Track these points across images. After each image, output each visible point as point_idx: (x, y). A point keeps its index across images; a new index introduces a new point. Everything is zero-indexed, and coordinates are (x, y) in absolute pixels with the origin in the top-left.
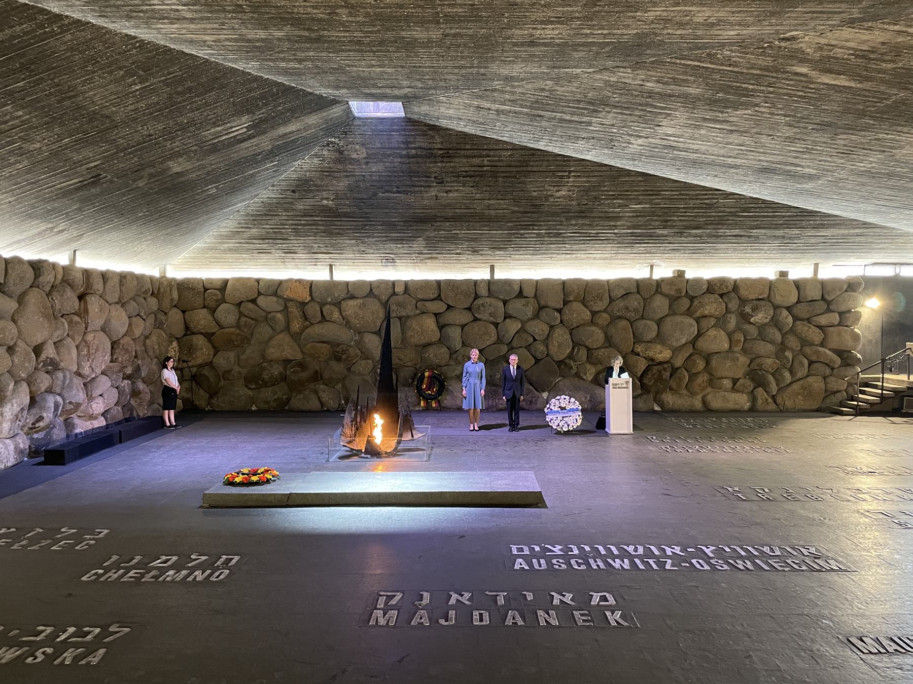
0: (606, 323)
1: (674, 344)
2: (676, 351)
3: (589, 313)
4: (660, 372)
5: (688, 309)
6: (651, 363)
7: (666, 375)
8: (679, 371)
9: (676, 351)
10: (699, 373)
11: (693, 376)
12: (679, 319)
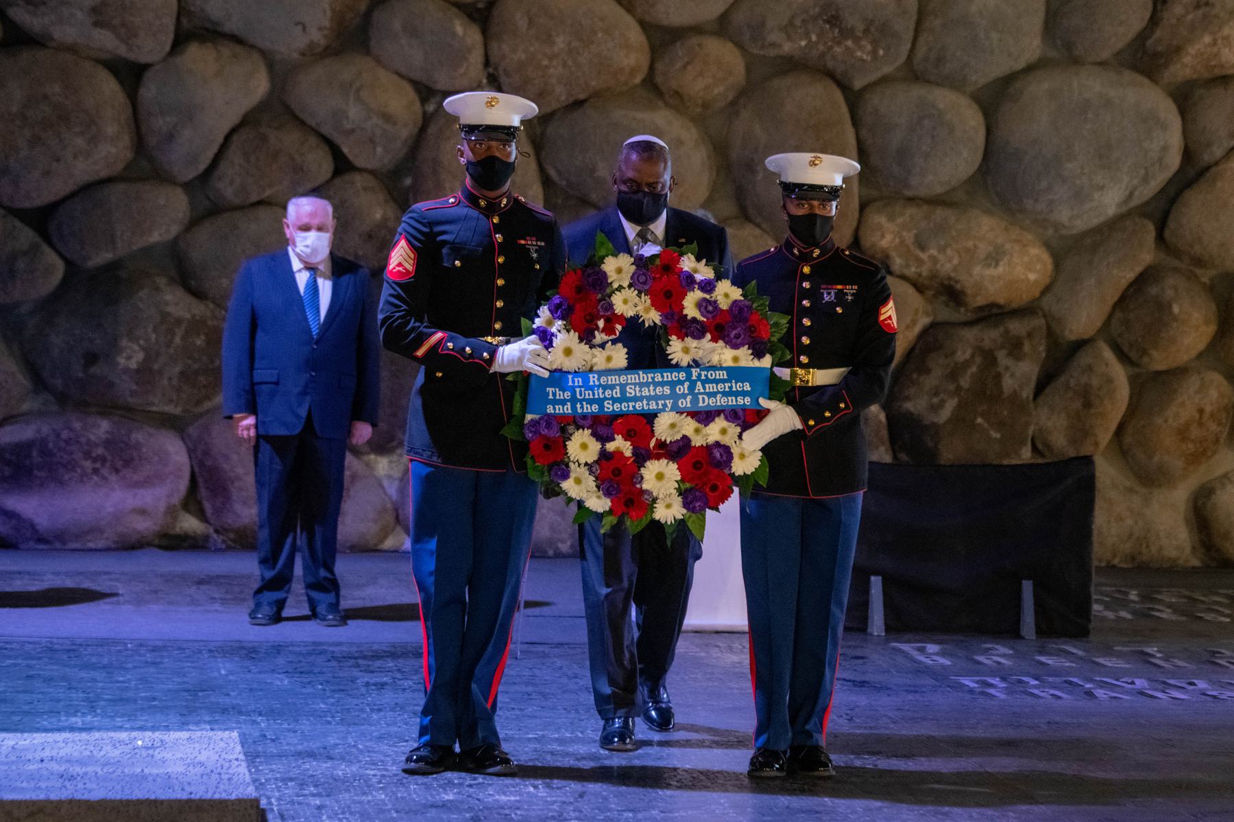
0: (721, 91)
1: (1063, 215)
2: (1070, 252)
3: (636, 35)
4: (989, 359)
5: (1143, 36)
6: (947, 314)
7: (1019, 374)
8: (1084, 359)
9: (1070, 252)
10: (1180, 372)
11: (1152, 387)
12: (1091, 85)
